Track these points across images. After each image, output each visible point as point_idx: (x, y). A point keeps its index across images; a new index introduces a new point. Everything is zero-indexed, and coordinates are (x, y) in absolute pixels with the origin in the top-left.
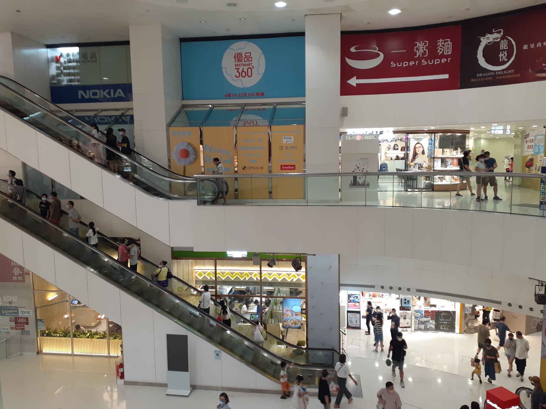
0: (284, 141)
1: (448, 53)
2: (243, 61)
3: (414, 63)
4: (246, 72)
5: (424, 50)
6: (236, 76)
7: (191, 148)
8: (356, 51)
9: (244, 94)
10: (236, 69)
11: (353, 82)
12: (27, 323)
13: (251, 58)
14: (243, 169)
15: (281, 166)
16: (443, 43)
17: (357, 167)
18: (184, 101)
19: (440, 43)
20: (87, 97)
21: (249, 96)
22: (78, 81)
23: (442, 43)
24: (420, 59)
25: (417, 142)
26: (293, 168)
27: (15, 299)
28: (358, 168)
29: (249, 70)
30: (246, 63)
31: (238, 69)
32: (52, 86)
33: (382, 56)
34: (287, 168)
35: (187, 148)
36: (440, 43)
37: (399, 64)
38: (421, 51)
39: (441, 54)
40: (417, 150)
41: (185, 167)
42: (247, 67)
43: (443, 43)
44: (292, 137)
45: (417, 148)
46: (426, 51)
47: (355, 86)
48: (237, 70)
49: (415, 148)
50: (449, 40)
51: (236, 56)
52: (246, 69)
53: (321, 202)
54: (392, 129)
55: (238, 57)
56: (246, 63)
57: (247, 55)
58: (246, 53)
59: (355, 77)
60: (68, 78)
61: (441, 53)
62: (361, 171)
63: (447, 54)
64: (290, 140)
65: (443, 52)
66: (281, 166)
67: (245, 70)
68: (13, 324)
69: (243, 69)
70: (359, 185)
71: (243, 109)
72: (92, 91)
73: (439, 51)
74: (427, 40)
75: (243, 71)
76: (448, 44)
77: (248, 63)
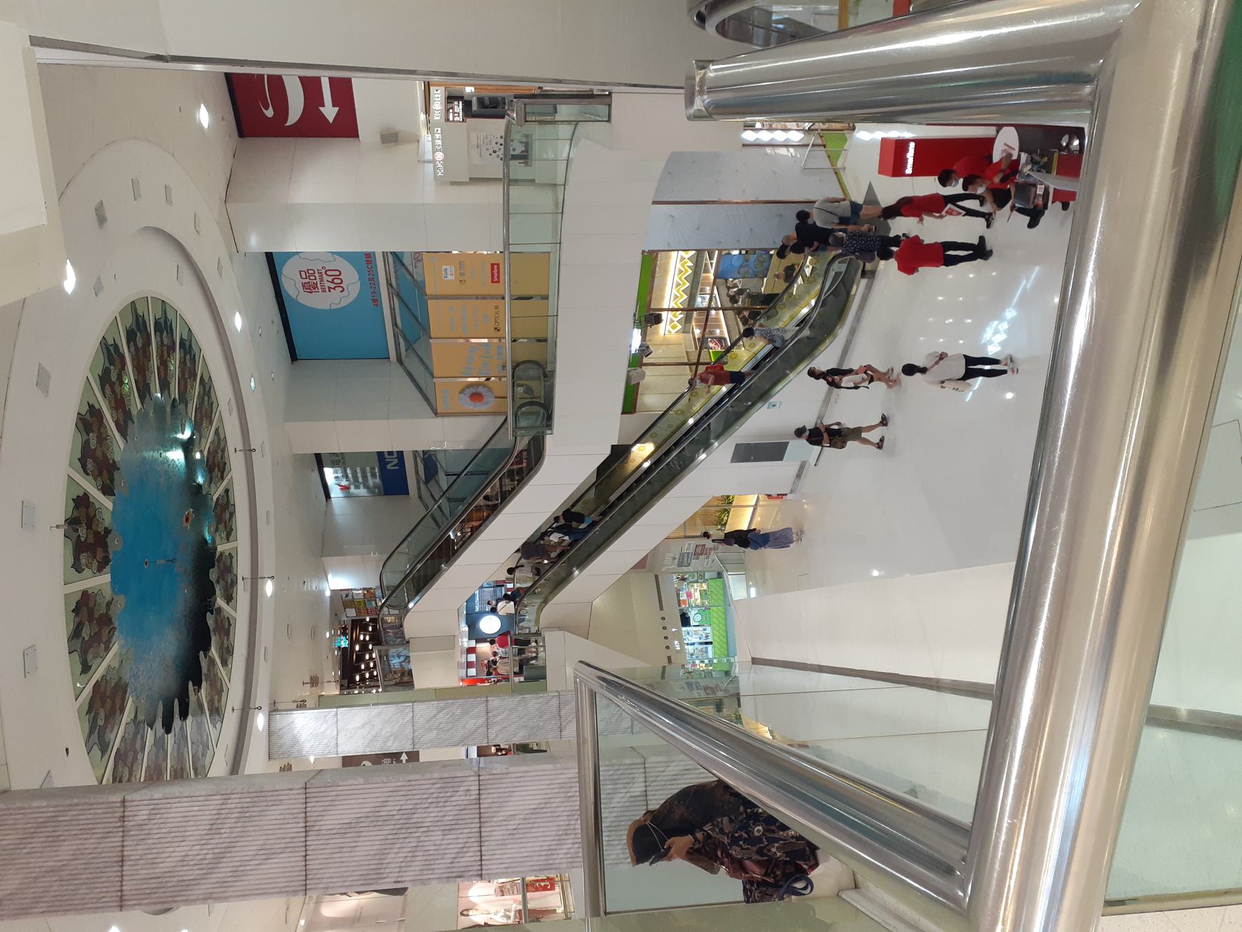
0: (450, 278)
10: (330, 291)
11: (330, 111)
12: (704, 545)
15: (493, 282)
17: (493, 154)
20: (396, 461)
22: (372, 469)
26: (496, 266)
28: (495, 152)
29: (328, 273)
31: (329, 288)
32: (383, 493)
34: (496, 274)
35: (468, 395)
41: (496, 398)
42: (324, 275)
44: (444, 267)
53: (556, 231)
55: (310, 288)
56: (318, 278)
57: (304, 276)
59: (321, 108)
60: (370, 478)
62: (502, 147)
66: (493, 282)
67: (330, 279)
70: (526, 151)
71: (395, 292)
75: (333, 282)
77: (317, 275)
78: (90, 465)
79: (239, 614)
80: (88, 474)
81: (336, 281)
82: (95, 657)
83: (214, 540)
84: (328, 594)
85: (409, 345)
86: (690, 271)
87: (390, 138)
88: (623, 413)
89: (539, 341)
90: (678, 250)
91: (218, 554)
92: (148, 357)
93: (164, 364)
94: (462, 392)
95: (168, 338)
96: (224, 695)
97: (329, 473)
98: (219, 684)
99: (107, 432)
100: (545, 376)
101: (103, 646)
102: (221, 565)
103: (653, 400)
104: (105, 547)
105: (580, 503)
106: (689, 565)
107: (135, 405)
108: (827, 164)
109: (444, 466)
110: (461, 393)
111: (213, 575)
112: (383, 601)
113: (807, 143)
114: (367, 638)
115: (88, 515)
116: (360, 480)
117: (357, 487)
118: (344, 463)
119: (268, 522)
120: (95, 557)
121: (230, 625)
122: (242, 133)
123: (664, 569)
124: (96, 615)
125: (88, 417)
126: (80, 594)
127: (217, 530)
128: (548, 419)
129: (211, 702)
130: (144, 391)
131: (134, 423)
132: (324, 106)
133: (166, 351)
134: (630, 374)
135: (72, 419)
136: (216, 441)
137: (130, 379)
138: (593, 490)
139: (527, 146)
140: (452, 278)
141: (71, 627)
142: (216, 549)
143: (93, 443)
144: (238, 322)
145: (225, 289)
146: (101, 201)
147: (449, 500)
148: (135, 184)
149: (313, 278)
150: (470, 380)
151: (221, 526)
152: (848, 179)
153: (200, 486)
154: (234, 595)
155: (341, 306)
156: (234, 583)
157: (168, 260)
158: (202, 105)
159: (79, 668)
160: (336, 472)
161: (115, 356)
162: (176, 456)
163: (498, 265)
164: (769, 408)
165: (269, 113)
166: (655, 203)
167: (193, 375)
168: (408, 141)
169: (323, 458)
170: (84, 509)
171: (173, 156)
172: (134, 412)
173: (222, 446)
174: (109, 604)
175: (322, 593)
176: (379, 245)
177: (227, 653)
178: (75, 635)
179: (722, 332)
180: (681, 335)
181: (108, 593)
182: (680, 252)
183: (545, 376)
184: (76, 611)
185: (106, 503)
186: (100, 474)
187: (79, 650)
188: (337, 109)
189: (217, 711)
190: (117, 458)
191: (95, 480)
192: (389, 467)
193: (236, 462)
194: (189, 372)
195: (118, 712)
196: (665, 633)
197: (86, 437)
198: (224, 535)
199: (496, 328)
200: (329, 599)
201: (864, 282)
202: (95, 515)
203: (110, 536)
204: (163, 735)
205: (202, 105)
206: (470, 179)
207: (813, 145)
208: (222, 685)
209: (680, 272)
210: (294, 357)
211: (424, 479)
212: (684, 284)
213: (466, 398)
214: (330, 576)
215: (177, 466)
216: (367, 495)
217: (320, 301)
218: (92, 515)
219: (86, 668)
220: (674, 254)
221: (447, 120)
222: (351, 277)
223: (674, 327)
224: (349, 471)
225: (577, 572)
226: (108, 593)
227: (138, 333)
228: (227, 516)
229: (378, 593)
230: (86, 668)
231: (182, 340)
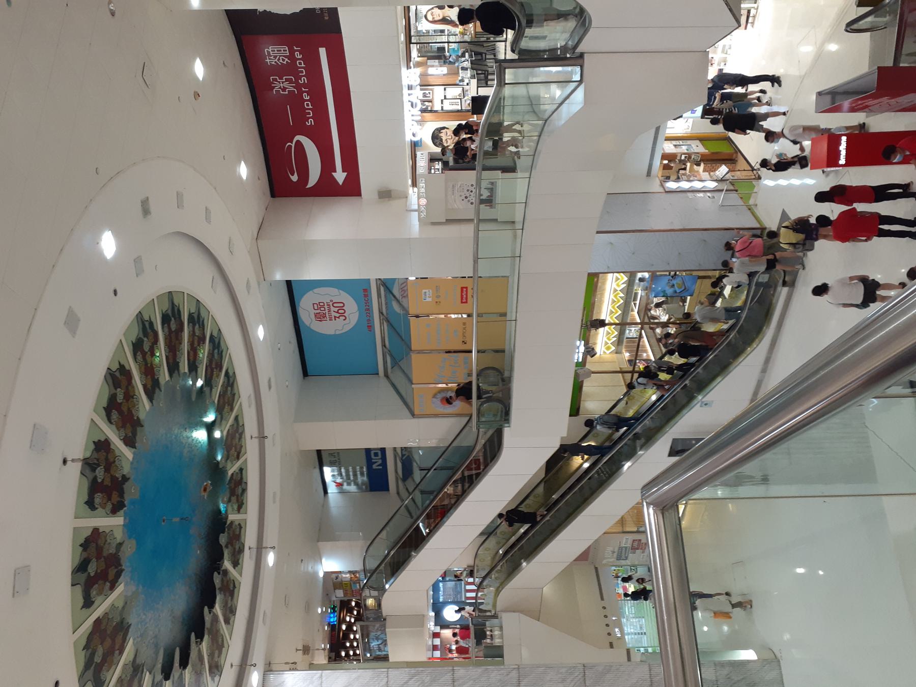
0: (429, 299)
1: (286, 51)
2: (324, 312)
3: (306, 94)
4: (338, 308)
5: (285, 82)
6: (344, 320)
7: (438, 394)
8: (296, 173)
9: (367, 312)
10: (335, 320)
11: (340, 176)
13: (319, 303)
14: (465, 343)
15: (462, 302)
16: (272, 58)
18: (380, 373)
19: (272, 62)
20: (380, 462)
21: (368, 306)
22: (362, 468)
23: (272, 59)
24: (298, 86)
25: (424, 19)
26: (465, 289)
27: (610, 549)
29: (335, 305)
30: (327, 309)
31: (335, 317)
33: (298, 138)
34: (465, 296)
35: (439, 399)
36: (272, 62)
37: (309, 114)
38: (286, 85)
39: (288, 59)
40: (437, 18)
43: (272, 58)
44: (424, 291)
45: (433, 18)
46: (285, 78)
47: (346, 173)
48: (337, 319)
49: (434, 22)
50: (266, 50)
51: (319, 319)
52: (333, 309)
54: (404, 70)
55: (320, 317)
56: (327, 309)
57: (316, 308)
58: (314, 309)
59: (333, 174)
60: (359, 476)
61: (286, 60)
63: (288, 52)
64: (427, 293)
65: (285, 57)
66: (462, 302)
67: (336, 309)
68: (638, 551)
69: (334, 311)
70: (491, 196)
71: (386, 318)
72: (373, 457)
73: (285, 63)
74: (270, 78)
75: (338, 312)
76: (272, 51)
77: (326, 307)
78: (115, 415)
79: (244, 579)
80: (111, 422)
81: (340, 311)
82: (100, 593)
83: (226, 511)
84: (321, 575)
85: (395, 363)
86: (622, 301)
87: (385, 195)
88: (570, 415)
89: (497, 351)
90: (613, 273)
91: (228, 522)
92: (179, 340)
93: (193, 352)
94: (434, 396)
95: (199, 331)
96: (224, 650)
97: (328, 472)
98: (220, 640)
99: (134, 391)
100: (503, 380)
101: (108, 584)
103: (594, 406)
104: (121, 494)
105: (531, 498)
106: (626, 558)
107: (164, 376)
108: (740, 202)
109: (419, 463)
110: (433, 397)
111: (223, 539)
112: (365, 582)
113: (721, 188)
114: (353, 620)
115: (107, 459)
116: (352, 478)
117: (349, 484)
118: (340, 464)
119: (274, 502)
120: (109, 499)
121: (234, 587)
122: (273, 194)
123: (604, 562)
124: (105, 553)
125: (117, 374)
126: (91, 530)
127: (229, 501)
128: (506, 414)
129: (211, 655)
130: (173, 367)
132: (336, 172)
133: (197, 340)
134: (577, 371)
135: (103, 371)
136: (235, 425)
137: (160, 355)
138: (542, 485)
139: (492, 190)
140: (430, 300)
141: (77, 562)
142: (227, 518)
143: (120, 398)
144: (261, 332)
145: (252, 305)
146: (148, 198)
147: (422, 492)
148: (179, 196)
149: (323, 309)
150: (440, 385)
151: (234, 499)
152: (760, 212)
153: (218, 463)
154: (240, 561)
155: (344, 331)
156: (241, 551)
157: (207, 272)
158: (243, 162)
159: (81, 601)
160: (333, 471)
161: (149, 330)
162: (201, 435)
163: (466, 288)
164: (701, 406)
165: (295, 178)
166: (598, 232)
167: (220, 367)
168: (400, 198)
169: (323, 453)
170: (104, 454)
171: (215, 189)
172: (162, 382)
173: (240, 431)
174: (120, 544)
175: (315, 574)
176: (373, 273)
177: (230, 612)
178: (81, 568)
179: (648, 356)
180: (615, 355)
181: (119, 535)
182: (615, 274)
183: (503, 380)
184: (85, 545)
185: (128, 453)
186: (124, 426)
187: (83, 584)
188: (346, 173)
189: (216, 669)
191: (119, 430)
192: (374, 467)
193: (251, 447)
194: (217, 364)
195: (117, 652)
196: (607, 621)
197: (113, 391)
198: (236, 507)
199: (463, 342)
200: (321, 580)
201: (785, 290)
202: (114, 462)
203: (127, 483)
204: (161, 681)
205: (243, 162)
206: (447, 220)
207: (726, 190)
208: (223, 641)
209: (614, 302)
210: (305, 373)
211: (401, 476)
212: (617, 312)
213: (437, 401)
214: (324, 560)
215: (200, 443)
216: (356, 491)
217: (328, 328)
218: (112, 460)
219: (88, 603)
220: (610, 276)
221: (430, 173)
222: (352, 308)
223: (608, 348)
224: (343, 470)
225: (524, 564)
226: (119, 535)
227: (173, 319)
228: (240, 491)
229: (362, 576)
230: (88, 603)
231: (212, 336)
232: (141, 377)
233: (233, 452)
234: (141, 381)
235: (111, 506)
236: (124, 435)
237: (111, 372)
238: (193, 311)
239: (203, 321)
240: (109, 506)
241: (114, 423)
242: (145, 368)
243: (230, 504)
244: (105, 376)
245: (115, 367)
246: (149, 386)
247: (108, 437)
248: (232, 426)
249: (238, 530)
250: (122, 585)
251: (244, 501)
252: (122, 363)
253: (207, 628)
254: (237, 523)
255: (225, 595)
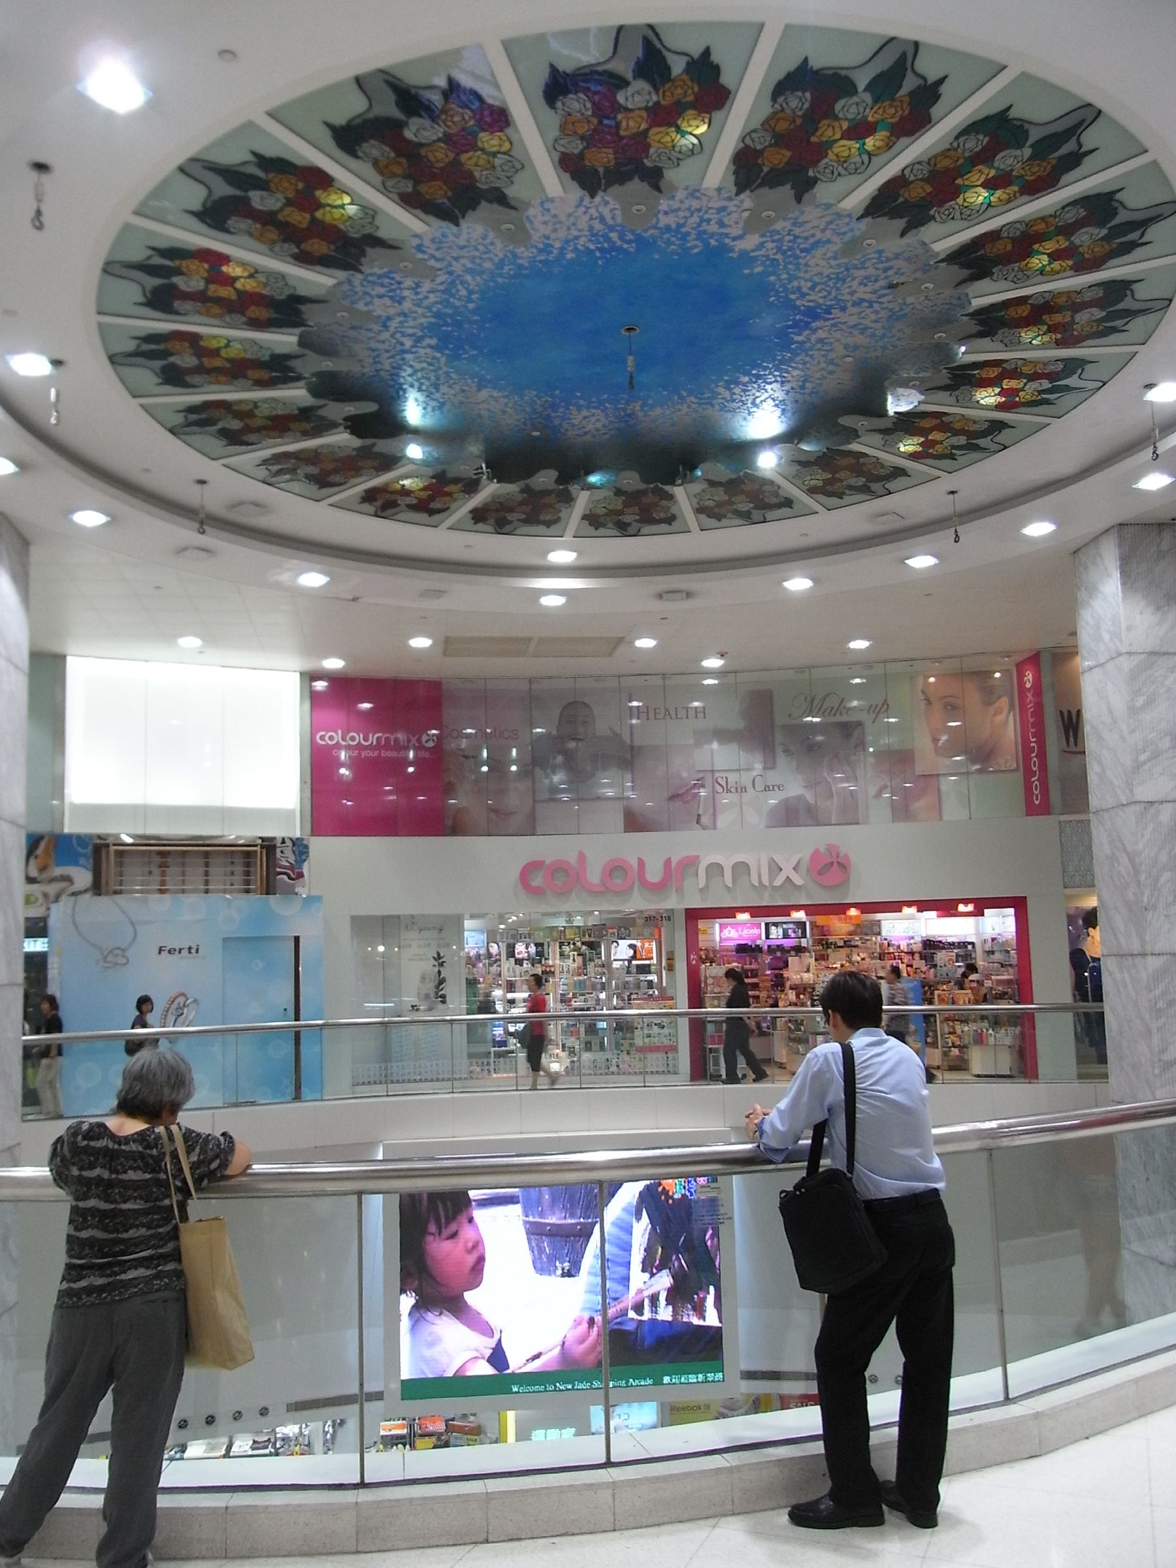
78: (799, 102)
80: (774, 97)
91: (667, 488)
102: (650, 499)
125: (909, 84)
131: (903, 234)
136: (883, 472)
172: (928, 232)
173: (875, 486)
186: (780, 140)
190: (824, 191)
232: (920, 163)
233: (818, 477)
234: (912, 165)
235: (576, 151)
236: (759, 147)
237: (910, 58)
238: (1141, 291)
239: (1115, 330)
240: (576, 147)
241: (777, 106)
242: (947, 170)
243: (705, 486)
244: (893, 39)
245: (928, 67)
246: (905, 195)
247: (736, 93)
248: (878, 462)
249: (662, 515)
250: (426, 228)
251: (725, 522)
252: (944, 89)
253: (374, 445)
254: (674, 510)
255: (522, 503)
